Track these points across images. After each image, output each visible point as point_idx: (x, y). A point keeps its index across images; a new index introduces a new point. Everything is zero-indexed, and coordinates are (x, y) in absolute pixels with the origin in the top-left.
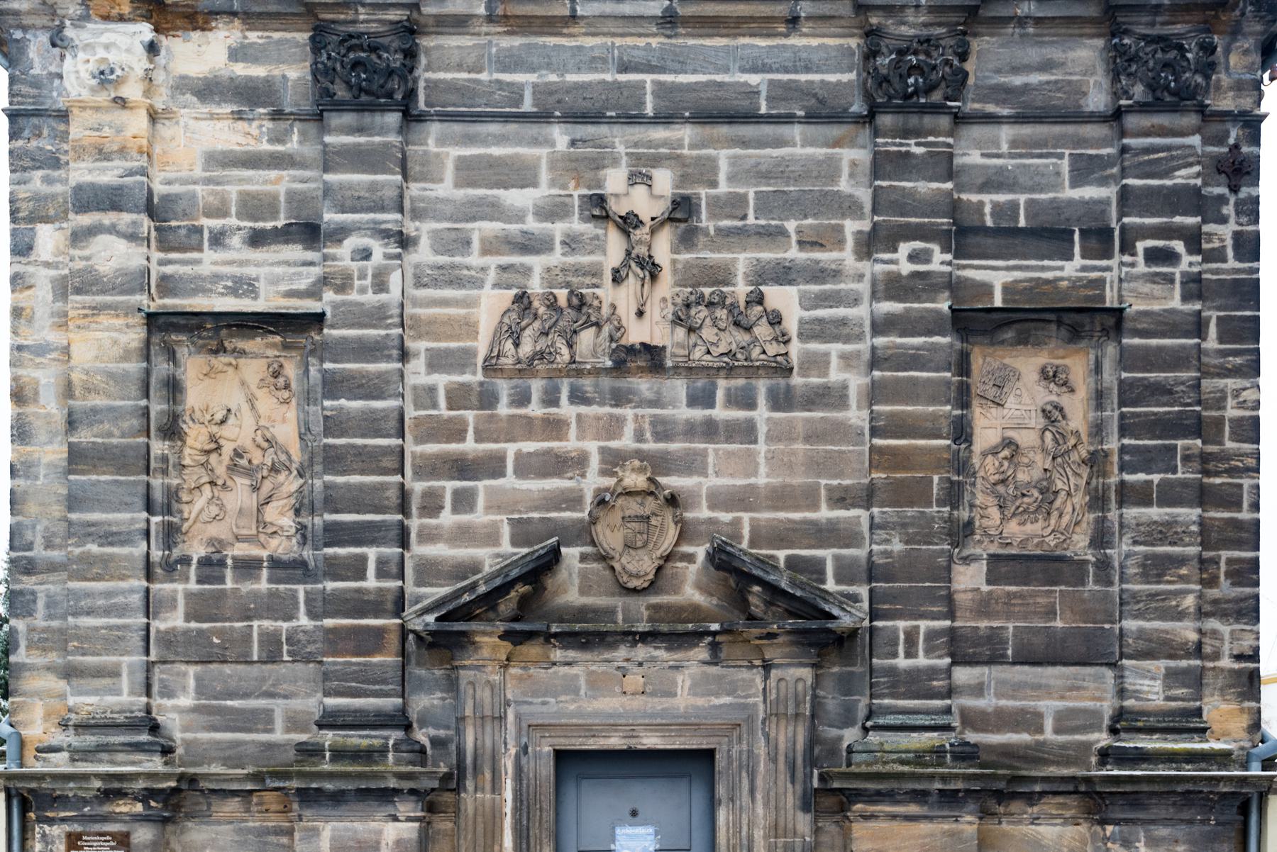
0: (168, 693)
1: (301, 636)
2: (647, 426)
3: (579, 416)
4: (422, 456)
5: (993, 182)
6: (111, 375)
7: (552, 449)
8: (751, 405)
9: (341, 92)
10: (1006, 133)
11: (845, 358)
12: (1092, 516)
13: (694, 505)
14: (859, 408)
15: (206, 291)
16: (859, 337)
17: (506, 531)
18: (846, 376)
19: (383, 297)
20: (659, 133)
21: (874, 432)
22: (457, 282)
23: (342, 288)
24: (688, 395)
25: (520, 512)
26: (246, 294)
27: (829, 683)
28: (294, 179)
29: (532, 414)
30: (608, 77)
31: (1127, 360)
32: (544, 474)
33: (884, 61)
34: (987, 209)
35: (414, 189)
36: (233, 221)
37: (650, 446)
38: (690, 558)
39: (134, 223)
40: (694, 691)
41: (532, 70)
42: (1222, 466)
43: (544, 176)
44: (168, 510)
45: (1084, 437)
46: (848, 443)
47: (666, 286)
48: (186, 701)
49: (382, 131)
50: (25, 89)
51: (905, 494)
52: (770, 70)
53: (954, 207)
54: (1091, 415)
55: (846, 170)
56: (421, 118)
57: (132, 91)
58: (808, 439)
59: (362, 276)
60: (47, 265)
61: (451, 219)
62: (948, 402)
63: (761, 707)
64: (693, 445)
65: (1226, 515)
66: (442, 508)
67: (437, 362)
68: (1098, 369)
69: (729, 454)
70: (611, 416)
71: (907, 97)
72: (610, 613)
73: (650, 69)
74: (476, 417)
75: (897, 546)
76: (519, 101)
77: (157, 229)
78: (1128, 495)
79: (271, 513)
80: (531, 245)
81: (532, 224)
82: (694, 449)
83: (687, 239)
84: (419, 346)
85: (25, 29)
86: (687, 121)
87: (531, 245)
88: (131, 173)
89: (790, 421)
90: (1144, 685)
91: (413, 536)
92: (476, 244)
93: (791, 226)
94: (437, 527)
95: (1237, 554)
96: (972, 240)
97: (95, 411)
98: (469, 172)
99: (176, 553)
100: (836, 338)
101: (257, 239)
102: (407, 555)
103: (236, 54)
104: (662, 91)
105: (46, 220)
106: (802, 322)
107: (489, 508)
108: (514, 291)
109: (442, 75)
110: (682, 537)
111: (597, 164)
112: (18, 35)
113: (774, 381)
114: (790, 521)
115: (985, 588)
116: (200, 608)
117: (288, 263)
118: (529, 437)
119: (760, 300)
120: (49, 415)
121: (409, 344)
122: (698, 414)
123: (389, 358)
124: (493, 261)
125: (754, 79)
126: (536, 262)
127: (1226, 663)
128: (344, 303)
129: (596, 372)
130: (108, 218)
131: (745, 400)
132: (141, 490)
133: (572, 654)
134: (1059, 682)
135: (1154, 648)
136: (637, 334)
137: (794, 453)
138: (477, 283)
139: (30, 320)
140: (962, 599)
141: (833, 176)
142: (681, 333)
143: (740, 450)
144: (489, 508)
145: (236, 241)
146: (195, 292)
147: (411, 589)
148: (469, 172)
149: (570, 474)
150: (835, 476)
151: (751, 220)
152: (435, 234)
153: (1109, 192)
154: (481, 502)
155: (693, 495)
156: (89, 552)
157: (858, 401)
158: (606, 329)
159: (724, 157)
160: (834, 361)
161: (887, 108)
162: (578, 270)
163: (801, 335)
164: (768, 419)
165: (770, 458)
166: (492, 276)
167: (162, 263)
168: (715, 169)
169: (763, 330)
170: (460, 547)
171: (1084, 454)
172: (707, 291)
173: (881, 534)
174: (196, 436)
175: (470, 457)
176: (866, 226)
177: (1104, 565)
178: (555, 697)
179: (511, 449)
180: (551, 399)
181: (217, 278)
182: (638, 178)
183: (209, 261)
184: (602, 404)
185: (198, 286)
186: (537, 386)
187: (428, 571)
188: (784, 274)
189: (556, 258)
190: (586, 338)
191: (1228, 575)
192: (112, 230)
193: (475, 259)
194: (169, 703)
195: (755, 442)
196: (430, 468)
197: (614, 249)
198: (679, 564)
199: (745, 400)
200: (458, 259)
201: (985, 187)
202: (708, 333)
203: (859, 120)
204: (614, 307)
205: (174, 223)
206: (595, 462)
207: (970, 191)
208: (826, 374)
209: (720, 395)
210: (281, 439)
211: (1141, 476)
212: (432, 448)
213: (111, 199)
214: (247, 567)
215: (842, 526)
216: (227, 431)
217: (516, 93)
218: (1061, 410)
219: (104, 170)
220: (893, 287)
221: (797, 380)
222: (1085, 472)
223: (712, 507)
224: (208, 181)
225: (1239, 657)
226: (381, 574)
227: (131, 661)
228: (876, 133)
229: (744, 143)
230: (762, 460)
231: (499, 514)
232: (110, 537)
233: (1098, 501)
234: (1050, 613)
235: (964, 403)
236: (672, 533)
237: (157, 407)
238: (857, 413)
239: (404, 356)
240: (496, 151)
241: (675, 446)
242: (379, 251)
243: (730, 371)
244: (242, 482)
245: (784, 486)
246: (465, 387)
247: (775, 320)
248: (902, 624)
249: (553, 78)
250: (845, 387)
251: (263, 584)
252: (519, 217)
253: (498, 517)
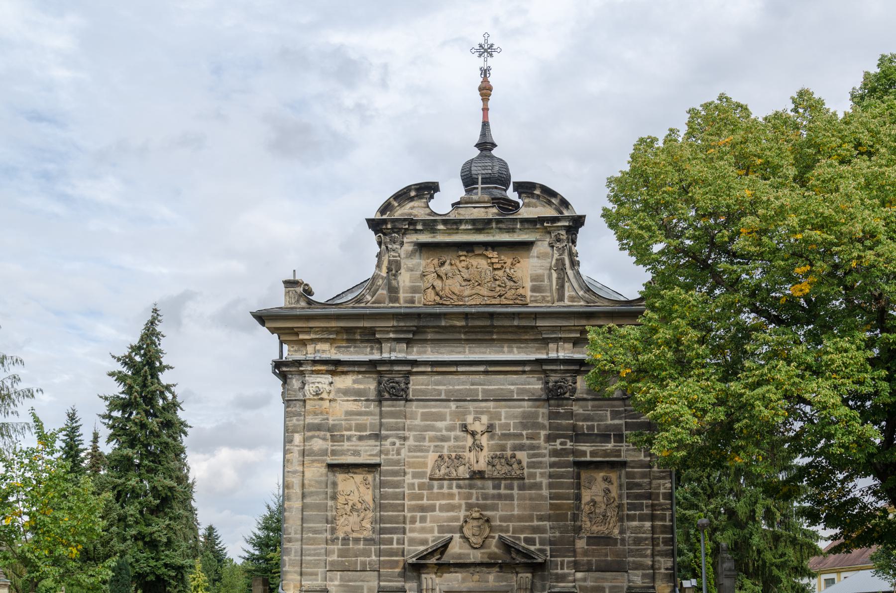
0: (331, 580)
1: (373, 563)
4: (411, 505)
5: (587, 418)
6: (317, 481)
8: (512, 489)
9: (387, 396)
10: (590, 403)
11: (541, 473)
12: (619, 524)
15: (345, 454)
16: (546, 468)
17: (436, 529)
19: (399, 457)
20: (484, 404)
21: (551, 498)
22: (421, 451)
23: (387, 454)
26: (357, 455)
28: (372, 419)
30: (468, 387)
31: (629, 475)
32: (448, 511)
33: (551, 384)
34: (585, 427)
35: (408, 422)
36: (353, 433)
37: (481, 502)
38: (493, 537)
39: (325, 435)
40: (494, 581)
41: (445, 385)
42: (660, 508)
43: (448, 418)
44: (332, 523)
45: (617, 499)
47: (485, 452)
48: (337, 583)
49: (399, 406)
50: (291, 392)
51: (563, 517)
52: (517, 385)
53: (574, 427)
54: (618, 492)
55: (541, 416)
56: (411, 400)
57: (325, 396)
59: (393, 451)
60: (297, 446)
61: (419, 431)
62: (573, 489)
65: (661, 523)
67: (415, 475)
68: (620, 477)
71: (558, 396)
72: (469, 554)
73: (481, 384)
75: (557, 534)
76: (440, 395)
77: (331, 435)
78: (631, 518)
79: (364, 523)
80: (444, 439)
81: (444, 433)
83: (492, 438)
84: (409, 470)
85: (292, 375)
86: (492, 401)
87: (444, 439)
88: (324, 420)
89: (524, 494)
90: (635, 578)
92: (427, 439)
93: (524, 433)
95: (665, 536)
96: (580, 437)
97: (312, 492)
98: (425, 417)
99: (335, 536)
100: (538, 468)
101: (361, 438)
103: (354, 382)
104: (484, 391)
105: (297, 432)
106: (528, 463)
107: (431, 522)
108: (439, 454)
109: (417, 387)
110: (491, 531)
111: (465, 414)
112: (290, 376)
115: (586, 547)
116: (343, 553)
117: (370, 446)
118: (443, 499)
119: (514, 456)
120: (296, 492)
121: (406, 470)
122: (496, 492)
123: (401, 476)
124: (433, 444)
125: (512, 387)
126: (446, 444)
127: (663, 571)
128: (387, 459)
129: (464, 479)
130: (317, 433)
131: (511, 488)
132: (325, 517)
133: (457, 569)
134: (610, 577)
135: (638, 566)
136: (476, 468)
137: (526, 504)
138: (428, 451)
139: (292, 463)
140: (579, 551)
141: (537, 418)
142: (490, 467)
144: (431, 522)
145: (354, 439)
146: (342, 455)
147: (406, 547)
148: (425, 417)
151: (512, 431)
152: (414, 436)
153: (622, 422)
154: (428, 519)
155: (494, 517)
156: (309, 537)
158: (467, 465)
159: (503, 411)
160: (538, 475)
161: (552, 399)
162: (458, 447)
163: (527, 467)
165: (518, 506)
166: (432, 448)
167: (332, 446)
168: (501, 416)
169: (515, 466)
171: (616, 504)
172: (498, 453)
173: (553, 531)
174: (341, 499)
176: (547, 432)
177: (623, 540)
179: (438, 503)
180: (450, 487)
181: (349, 450)
182: (475, 419)
183: (346, 445)
184: (466, 489)
185: (342, 453)
186: (446, 483)
187: (412, 542)
188: (521, 448)
189: (452, 443)
190: (461, 468)
191: (662, 542)
192: (318, 437)
193: (427, 444)
194: (332, 583)
196: (413, 509)
197: (470, 441)
199: (511, 488)
200: (422, 443)
201: (585, 420)
202: (498, 467)
203: (544, 400)
204: (469, 458)
205: (336, 433)
207: (579, 421)
208: (535, 479)
209: (503, 485)
210: (367, 500)
211: (633, 512)
212: (413, 503)
213: (318, 427)
214: (357, 540)
216: (350, 497)
217: (439, 392)
218: (609, 491)
219: (316, 419)
220: (555, 453)
221: (527, 481)
222: (616, 510)
223: (500, 521)
224: (346, 420)
225: (667, 569)
226: (398, 543)
227: (321, 570)
228: (549, 406)
229: (510, 407)
230: (516, 506)
232: (315, 532)
233: (621, 519)
234: (606, 555)
235: (579, 489)
236: (488, 530)
237: (329, 490)
239: (405, 473)
240: (433, 410)
241: (489, 502)
242: (398, 443)
243: (505, 479)
244: (355, 514)
246: (423, 483)
247: (520, 462)
248: (559, 559)
249: (451, 387)
250: (541, 483)
251: (361, 546)
252: (440, 430)
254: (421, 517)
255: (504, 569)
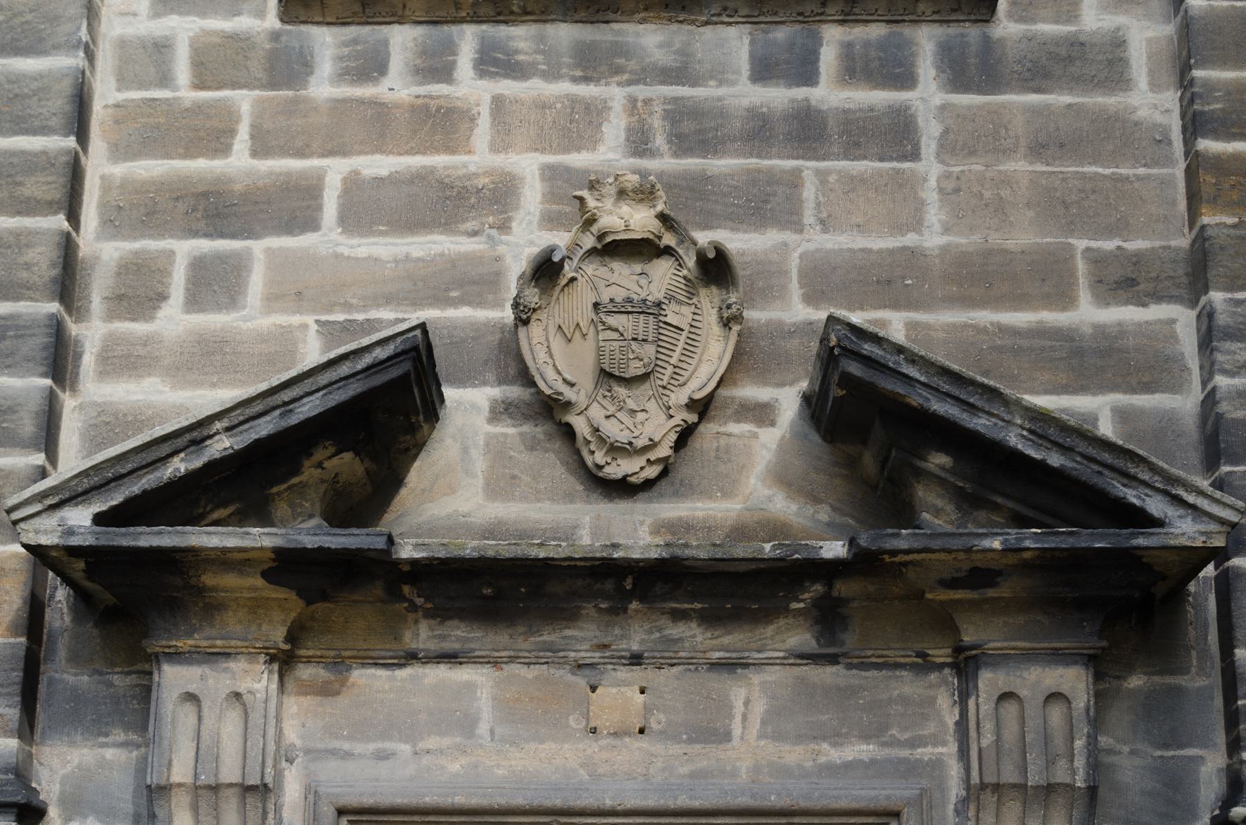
2: (657, 122)
3: (498, 104)
7: (432, 170)
8: (904, 78)
13: (771, 290)
14: (1155, 86)
18: (1121, 20)
24: (752, 56)
25: (348, 307)
27: (1120, 716)
29: (388, 97)
37: (665, 163)
38: (762, 414)
46: (1136, 161)
58: (1037, 150)
63: (954, 770)
64: (766, 162)
66: (163, 297)
69: (853, 183)
70: (574, 100)
74: (259, 103)
82: (770, 171)
89: (994, 112)
91: (88, 361)
94: (147, 341)
102: (68, 403)
107: (272, 300)
113: (953, 30)
114: (1003, 329)
137: (1007, 181)
143: (880, 173)
144: (272, 300)
149: (470, 225)
150: (1110, 232)
157: (1151, 73)
164: (943, 108)
165: (951, 192)
170: (198, 384)
175: (238, 187)
178: (410, 738)
179: (335, 171)
184: (552, 75)
195: (915, 156)
198: (734, 428)
206: (532, 198)
208: (1072, 16)
209: (828, 57)
215: (1131, 342)
230: (930, 195)
231: (299, 311)
238: (1152, 98)
241: (723, 165)
245: (988, 253)
246: (238, 42)
250: (1118, 43)
253: (296, 320)
254: (201, 270)
255: (850, 639)
